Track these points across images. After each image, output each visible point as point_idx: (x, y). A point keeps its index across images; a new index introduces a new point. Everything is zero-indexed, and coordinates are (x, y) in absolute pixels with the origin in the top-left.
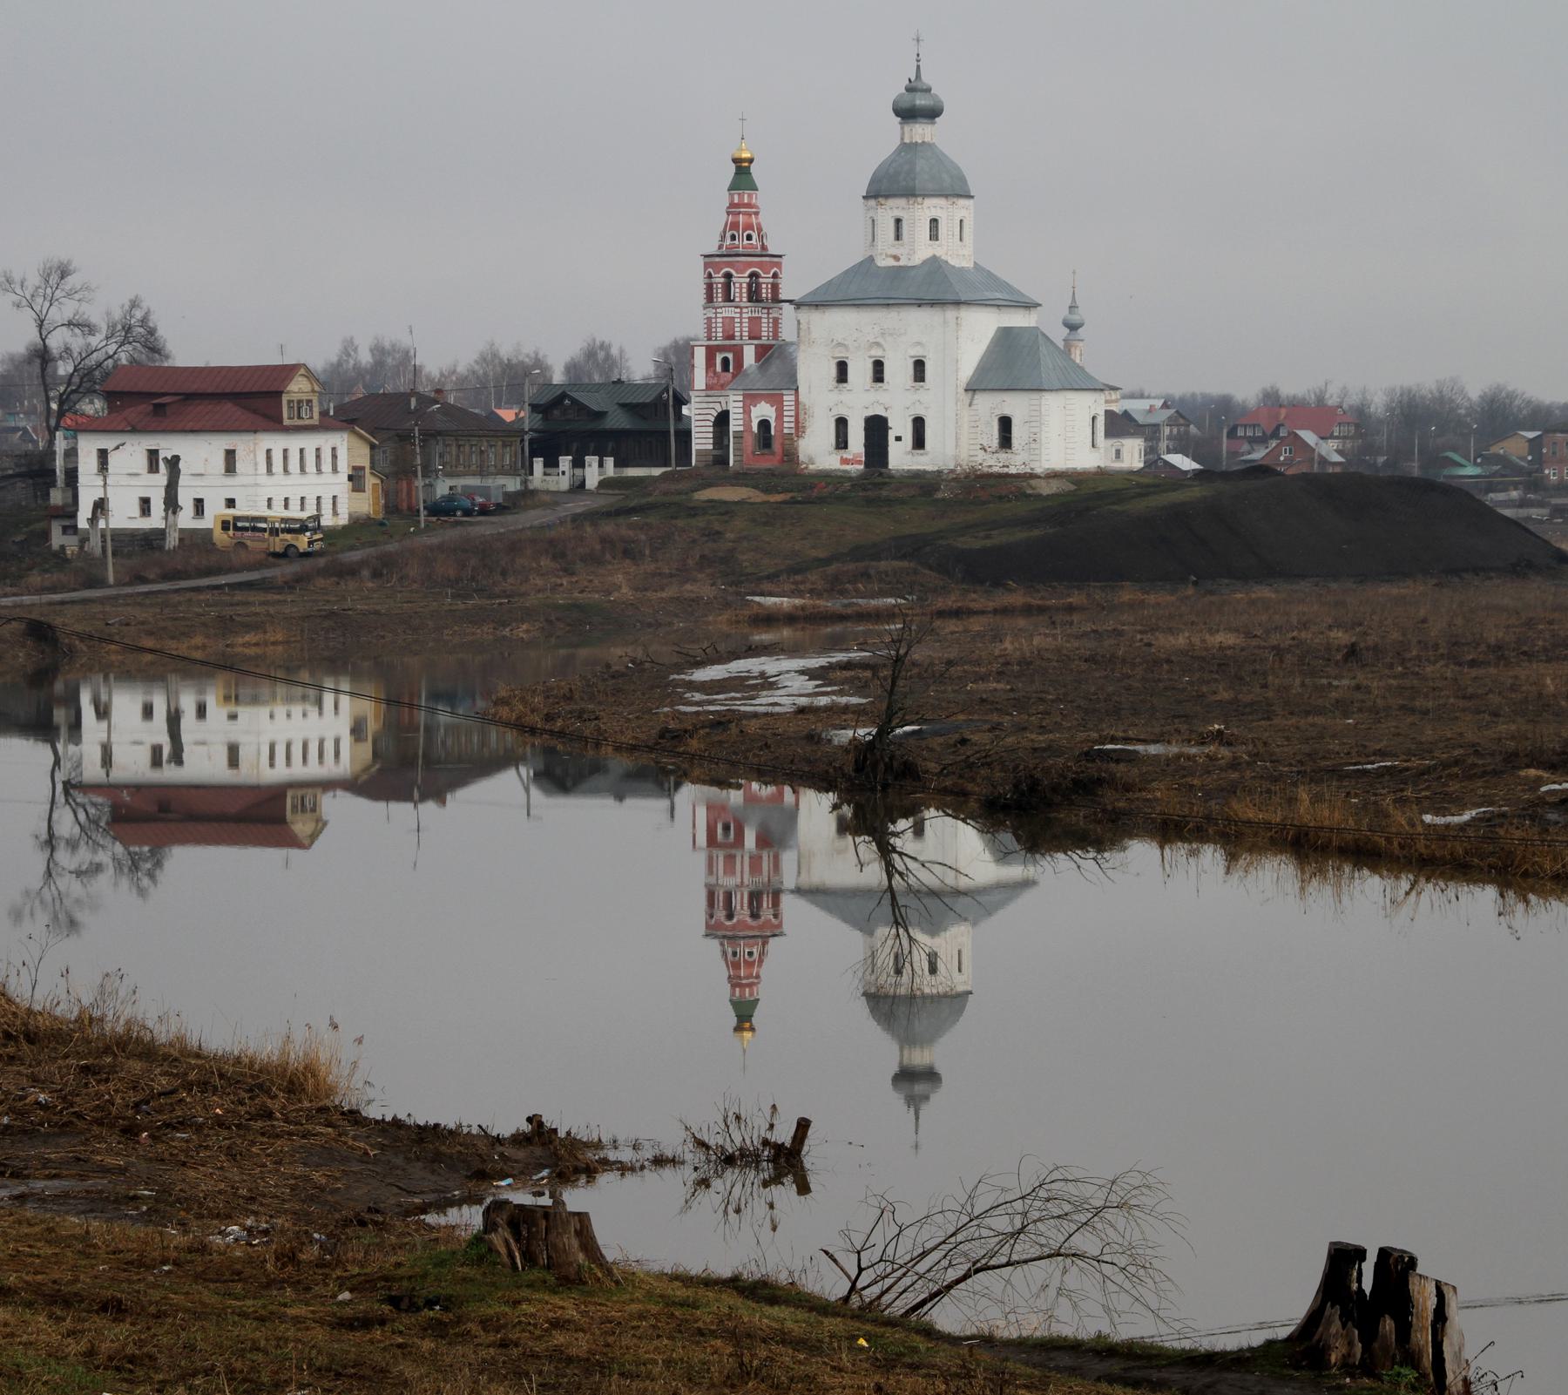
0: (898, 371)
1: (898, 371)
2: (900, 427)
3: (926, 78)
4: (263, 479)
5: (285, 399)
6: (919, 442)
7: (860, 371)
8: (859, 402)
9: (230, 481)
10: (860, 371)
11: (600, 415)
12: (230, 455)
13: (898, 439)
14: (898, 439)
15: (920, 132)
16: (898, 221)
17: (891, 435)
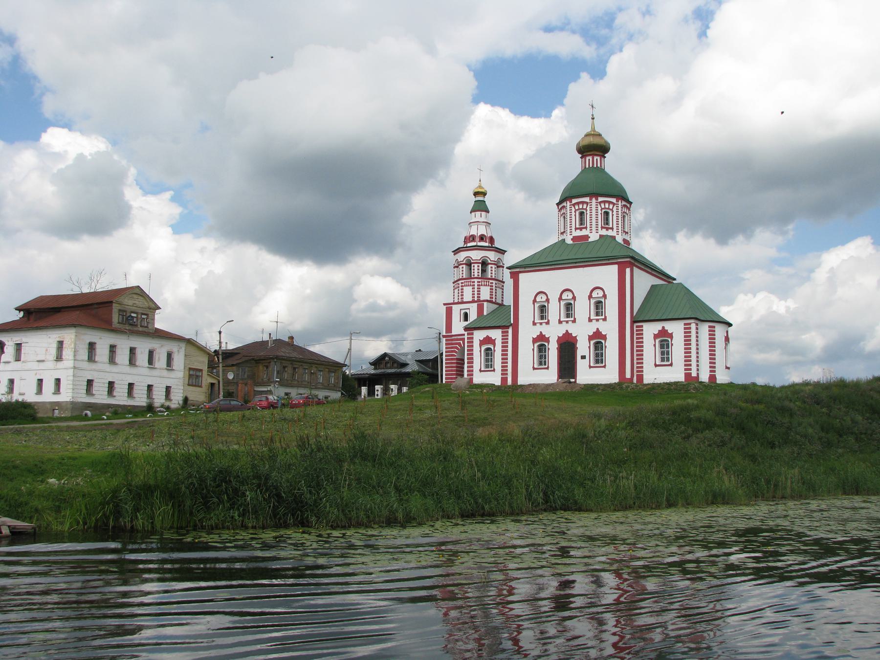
0: (582, 308)
1: (582, 308)
2: (583, 347)
3: (598, 129)
4: (86, 365)
5: (115, 308)
6: (599, 360)
7: (555, 310)
8: (554, 332)
9: (59, 363)
10: (555, 310)
11: (405, 365)
12: (61, 344)
13: (583, 357)
14: (583, 357)
15: (593, 160)
16: (582, 214)
17: (579, 354)
